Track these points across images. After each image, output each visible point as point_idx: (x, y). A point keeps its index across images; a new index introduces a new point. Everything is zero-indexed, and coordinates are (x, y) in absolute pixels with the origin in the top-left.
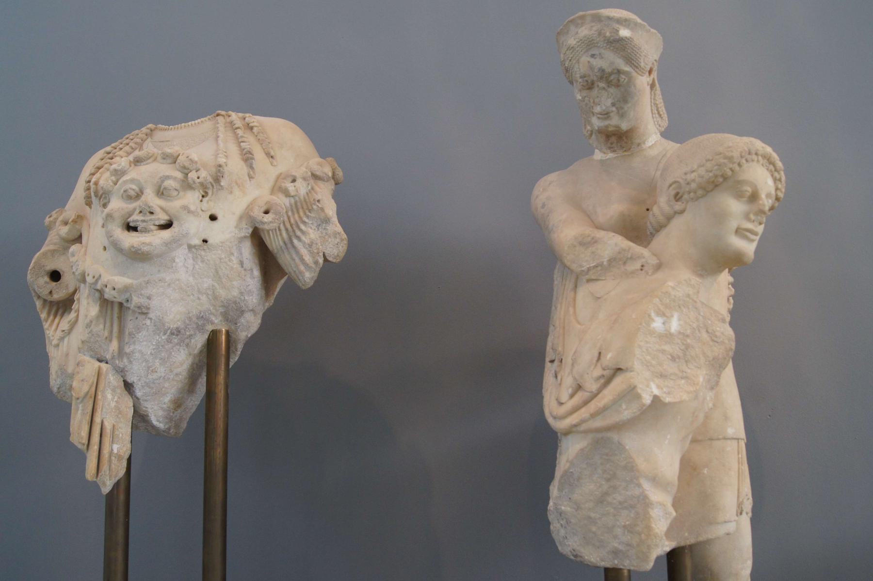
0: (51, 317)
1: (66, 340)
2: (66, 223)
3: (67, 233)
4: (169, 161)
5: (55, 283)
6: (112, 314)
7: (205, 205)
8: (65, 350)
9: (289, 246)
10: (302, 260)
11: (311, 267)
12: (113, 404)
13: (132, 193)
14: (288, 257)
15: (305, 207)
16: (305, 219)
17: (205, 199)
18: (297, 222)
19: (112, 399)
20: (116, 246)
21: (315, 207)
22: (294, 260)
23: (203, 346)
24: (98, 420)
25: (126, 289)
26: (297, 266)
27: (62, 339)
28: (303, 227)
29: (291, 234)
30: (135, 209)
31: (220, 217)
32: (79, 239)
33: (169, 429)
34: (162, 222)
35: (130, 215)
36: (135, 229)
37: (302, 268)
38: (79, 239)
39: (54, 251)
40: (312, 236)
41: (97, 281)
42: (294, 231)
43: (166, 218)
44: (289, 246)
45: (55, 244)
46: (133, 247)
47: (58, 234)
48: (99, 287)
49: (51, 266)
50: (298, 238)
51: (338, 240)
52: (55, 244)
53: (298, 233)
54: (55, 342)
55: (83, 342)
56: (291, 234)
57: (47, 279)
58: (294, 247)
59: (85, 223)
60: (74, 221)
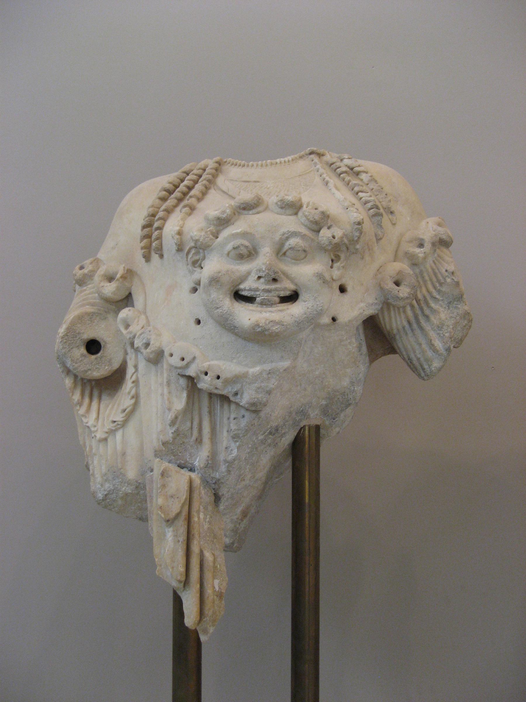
0: (87, 400)
1: (119, 435)
2: (110, 279)
3: (114, 293)
4: (289, 211)
5: (93, 357)
6: (200, 409)
7: (336, 273)
8: (119, 447)
9: (415, 326)
10: (431, 345)
11: (440, 355)
12: (206, 526)
13: (244, 251)
14: (412, 339)
15: (434, 279)
16: (435, 294)
17: (336, 265)
18: (424, 297)
19: (205, 519)
20: (227, 325)
21: (449, 280)
22: (420, 345)
23: (288, 445)
24: (195, 549)
25: (236, 379)
26: (423, 352)
27: (112, 432)
28: (433, 305)
29: (419, 312)
30: (249, 273)
31: (349, 288)
32: (127, 300)
33: (233, 543)
34: (288, 293)
35: (243, 279)
36: (250, 300)
37: (430, 354)
38: (127, 300)
39: (93, 314)
40: (443, 316)
41: (188, 366)
42: (422, 309)
43: (292, 287)
44: (415, 326)
45: (93, 305)
46: (258, 325)
47: (99, 293)
48: (191, 372)
49: (89, 334)
50: (427, 317)
51: (466, 322)
52: (93, 305)
53: (427, 312)
54: (100, 435)
55: (164, 444)
56: (419, 312)
57: (83, 350)
58: (421, 328)
59: (136, 280)
60: (123, 277)
